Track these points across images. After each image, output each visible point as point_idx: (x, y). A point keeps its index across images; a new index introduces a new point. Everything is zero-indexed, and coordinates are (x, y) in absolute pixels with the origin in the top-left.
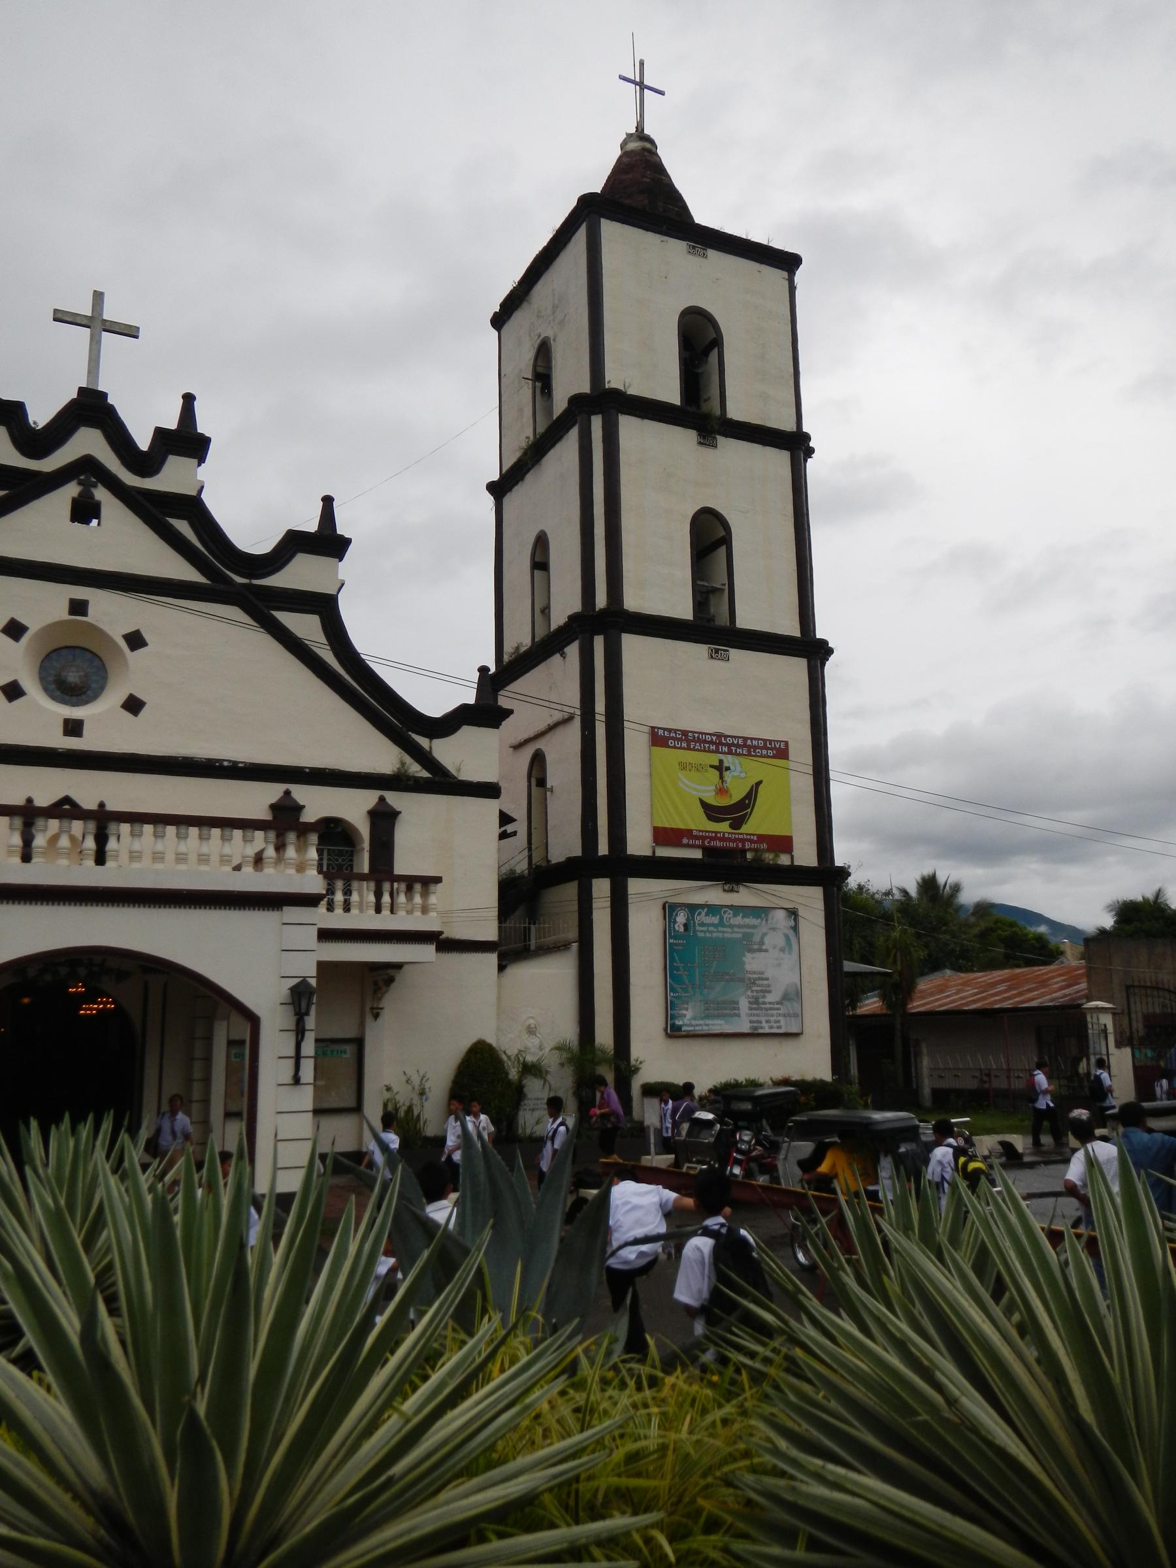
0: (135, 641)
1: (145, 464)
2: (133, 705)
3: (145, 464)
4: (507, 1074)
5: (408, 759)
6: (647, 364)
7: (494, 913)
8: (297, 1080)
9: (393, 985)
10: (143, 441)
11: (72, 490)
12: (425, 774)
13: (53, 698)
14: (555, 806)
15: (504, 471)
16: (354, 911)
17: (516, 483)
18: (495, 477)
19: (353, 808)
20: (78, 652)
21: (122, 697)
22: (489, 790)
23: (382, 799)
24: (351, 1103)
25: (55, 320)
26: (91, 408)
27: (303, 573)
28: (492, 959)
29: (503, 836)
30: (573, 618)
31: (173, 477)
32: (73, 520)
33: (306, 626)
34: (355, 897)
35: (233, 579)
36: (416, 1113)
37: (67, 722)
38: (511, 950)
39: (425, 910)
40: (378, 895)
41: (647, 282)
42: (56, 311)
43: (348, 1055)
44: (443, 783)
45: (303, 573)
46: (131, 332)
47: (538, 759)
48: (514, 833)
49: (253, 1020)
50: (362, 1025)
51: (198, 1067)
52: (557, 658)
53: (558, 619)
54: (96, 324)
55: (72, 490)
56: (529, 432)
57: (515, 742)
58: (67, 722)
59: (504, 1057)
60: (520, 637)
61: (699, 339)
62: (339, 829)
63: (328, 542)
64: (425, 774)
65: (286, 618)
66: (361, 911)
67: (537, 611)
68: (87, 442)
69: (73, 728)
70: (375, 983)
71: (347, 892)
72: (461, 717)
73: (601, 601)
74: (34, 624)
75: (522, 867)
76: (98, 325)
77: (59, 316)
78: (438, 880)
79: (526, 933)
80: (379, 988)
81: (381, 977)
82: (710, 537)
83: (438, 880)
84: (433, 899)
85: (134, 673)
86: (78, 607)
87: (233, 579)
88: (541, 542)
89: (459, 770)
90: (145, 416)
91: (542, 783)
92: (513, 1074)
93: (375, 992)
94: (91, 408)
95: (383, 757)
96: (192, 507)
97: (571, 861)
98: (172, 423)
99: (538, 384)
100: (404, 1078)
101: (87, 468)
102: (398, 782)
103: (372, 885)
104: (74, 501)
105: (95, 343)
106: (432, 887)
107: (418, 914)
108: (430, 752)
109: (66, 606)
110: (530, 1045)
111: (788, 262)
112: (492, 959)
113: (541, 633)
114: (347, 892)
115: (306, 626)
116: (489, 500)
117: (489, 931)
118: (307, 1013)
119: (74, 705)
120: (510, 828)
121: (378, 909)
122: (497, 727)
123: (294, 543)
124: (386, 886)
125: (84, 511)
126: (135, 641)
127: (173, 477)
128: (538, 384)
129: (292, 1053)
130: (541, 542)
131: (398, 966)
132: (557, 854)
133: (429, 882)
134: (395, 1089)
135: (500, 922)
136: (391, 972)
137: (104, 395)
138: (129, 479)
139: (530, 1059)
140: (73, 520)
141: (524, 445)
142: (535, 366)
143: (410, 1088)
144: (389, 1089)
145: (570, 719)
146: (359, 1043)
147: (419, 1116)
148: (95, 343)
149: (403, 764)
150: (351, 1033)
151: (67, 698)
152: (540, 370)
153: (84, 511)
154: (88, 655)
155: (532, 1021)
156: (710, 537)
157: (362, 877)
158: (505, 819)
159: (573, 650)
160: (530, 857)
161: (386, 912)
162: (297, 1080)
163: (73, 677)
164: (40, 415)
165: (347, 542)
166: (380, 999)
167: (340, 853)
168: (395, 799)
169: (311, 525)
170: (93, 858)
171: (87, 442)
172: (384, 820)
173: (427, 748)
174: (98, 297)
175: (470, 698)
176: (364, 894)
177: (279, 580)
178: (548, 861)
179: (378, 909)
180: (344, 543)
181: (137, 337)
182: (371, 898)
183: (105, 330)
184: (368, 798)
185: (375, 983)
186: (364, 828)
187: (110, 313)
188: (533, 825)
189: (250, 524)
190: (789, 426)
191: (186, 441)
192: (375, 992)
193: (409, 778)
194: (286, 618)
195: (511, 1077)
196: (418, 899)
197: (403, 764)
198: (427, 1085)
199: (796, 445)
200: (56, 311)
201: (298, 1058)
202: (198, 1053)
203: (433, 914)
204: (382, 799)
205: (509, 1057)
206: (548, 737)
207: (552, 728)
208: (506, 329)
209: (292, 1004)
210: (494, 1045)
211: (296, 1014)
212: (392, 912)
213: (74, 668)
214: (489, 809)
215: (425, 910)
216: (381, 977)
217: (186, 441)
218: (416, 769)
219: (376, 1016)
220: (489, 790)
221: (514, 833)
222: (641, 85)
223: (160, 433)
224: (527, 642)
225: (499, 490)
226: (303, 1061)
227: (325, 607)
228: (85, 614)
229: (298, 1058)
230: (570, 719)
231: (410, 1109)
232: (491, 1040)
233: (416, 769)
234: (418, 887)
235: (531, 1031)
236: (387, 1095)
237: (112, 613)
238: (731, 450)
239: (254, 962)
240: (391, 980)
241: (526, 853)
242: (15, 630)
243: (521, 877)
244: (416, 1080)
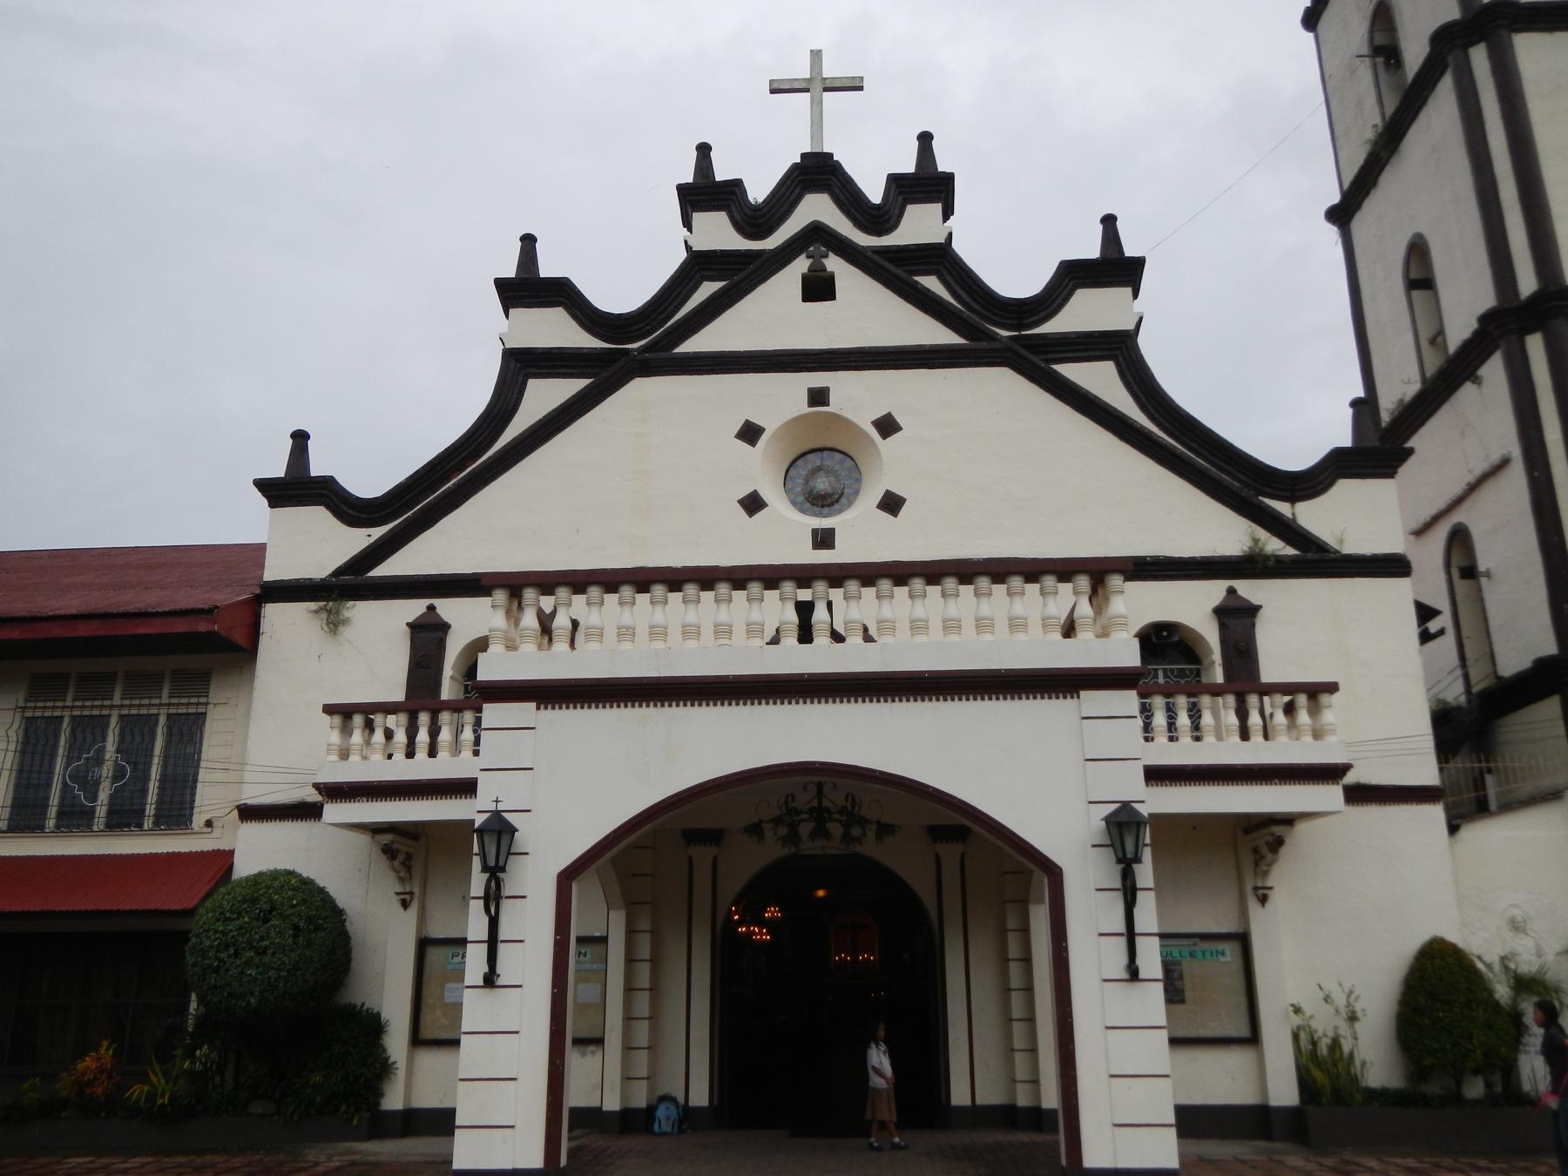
1: (878, 218)
2: (891, 504)
3: (878, 218)
4: (1491, 992)
5: (1262, 534)
7: (1428, 742)
8: (1133, 974)
9: (1284, 851)
10: (874, 192)
11: (801, 265)
12: (1290, 551)
13: (803, 511)
14: (1496, 597)
15: (1346, 185)
16: (1209, 739)
17: (1367, 194)
18: (1335, 198)
19: (1192, 606)
20: (826, 453)
21: (878, 496)
22: (1392, 566)
23: (1231, 591)
24: (1244, 1032)
25: (773, 91)
26: (817, 172)
27: (1089, 311)
28: (1435, 813)
29: (1426, 637)
30: (1486, 319)
31: (918, 225)
32: (805, 299)
33: (1101, 379)
34: (1207, 719)
35: (997, 332)
36: (1346, 1049)
37: (815, 532)
38: (1465, 801)
39: (1317, 734)
40: (1242, 714)
42: (771, 82)
43: (1228, 958)
44: (1317, 560)
45: (1089, 311)
46: (855, 86)
47: (1460, 539)
48: (1442, 632)
49: (1054, 873)
50: (1244, 914)
51: (1015, 969)
52: (1468, 389)
53: (1459, 329)
54: (819, 85)
56: (1378, 121)
57: (1415, 525)
58: (815, 532)
59: (1480, 966)
60: (1400, 383)
62: (1176, 639)
63: (1116, 268)
64: (1290, 551)
66: (1219, 738)
67: (1425, 344)
68: (817, 208)
69: (824, 539)
70: (1256, 851)
71: (1195, 713)
72: (1338, 466)
73: (1527, 283)
74: (770, 423)
75: (1455, 693)
76: (818, 86)
77: (775, 86)
78: (1332, 688)
79: (1479, 784)
80: (1262, 857)
81: (1260, 839)
83: (1332, 688)
84: (1328, 717)
85: (891, 465)
86: (818, 397)
87: (997, 332)
88: (1418, 250)
89: (1341, 541)
91: (1470, 572)
92: (1502, 992)
93: (1257, 863)
94: (817, 172)
95: (1222, 531)
96: (941, 257)
97: (1542, 665)
98: (907, 164)
99: (1380, 60)
100: (1321, 995)
101: (817, 235)
102: (1252, 566)
103: (1231, 699)
104: (805, 278)
105: (817, 106)
106: (1325, 699)
107: (1308, 739)
108: (1294, 520)
109: (804, 397)
110: (1520, 949)
112: (1435, 813)
113: (1433, 364)
114: (1195, 713)
115: (1101, 379)
116: (1332, 233)
117: (1426, 773)
118: (1137, 859)
119: (826, 516)
120: (1433, 626)
121: (1245, 735)
122: (1391, 475)
123: (1073, 276)
124: (1253, 700)
125: (818, 288)
126: (887, 426)
128: (1380, 60)
129: (1120, 927)
130: (1418, 250)
131: (1288, 820)
132: (1514, 658)
133: (1317, 692)
134: (1308, 1011)
135: (1440, 761)
136: (1278, 830)
137: (830, 155)
139: (1527, 964)
140: (805, 299)
141: (1370, 134)
142: (1371, 39)
143: (1330, 1009)
144: (1297, 1010)
145: (1504, 463)
146: (1243, 940)
147: (1351, 1055)
148: (817, 106)
149: (1256, 541)
150: (1226, 924)
151: (817, 509)
152: (1380, 39)
153: (818, 288)
154: (838, 456)
155: (1516, 912)
157: (1216, 691)
158: (1425, 613)
159: (1494, 370)
160: (1466, 677)
161: (1257, 738)
162: (1133, 974)
163: (822, 484)
164: (758, 191)
165: (1138, 264)
166: (1266, 874)
167: (1182, 673)
168: (1249, 589)
169: (1091, 250)
170: (795, 634)
171: (817, 208)
172: (1237, 619)
173: (1289, 515)
174: (816, 55)
175: (1345, 439)
176: (1220, 713)
177: (1058, 324)
178: (1499, 678)
179: (1245, 735)
180: (1138, 264)
181: (860, 88)
182: (1232, 719)
183: (826, 89)
184: (1213, 592)
185: (1256, 851)
186: (1210, 633)
187: (830, 70)
188: (1465, 633)
189: (1012, 266)
191: (928, 184)
192: (1257, 863)
193: (1267, 557)
195: (1497, 996)
196: (1303, 717)
197: (1256, 541)
198: (1358, 1007)
200: (771, 82)
201: (1131, 935)
202: (1014, 950)
203: (1331, 739)
204: (1231, 591)
205: (1489, 966)
206: (1468, 503)
207: (1473, 488)
208: (1325, 22)
209: (1112, 845)
210: (1461, 945)
211: (1119, 861)
212: (1266, 737)
213: (823, 470)
214: (1396, 595)
215: (1317, 734)
216: (1260, 839)
217: (928, 184)
218: (1275, 546)
219: (1263, 900)
220: (1392, 566)
221: (1442, 632)
223: (895, 181)
224: (1413, 389)
225: (1341, 216)
226: (1139, 941)
227: (1119, 347)
228: (827, 404)
229: (1131, 935)
230: (1504, 463)
231: (1335, 1044)
232: (1453, 937)
233: (1275, 546)
234: (1302, 699)
235: (1517, 926)
236: (1297, 1020)
239: (1044, 778)
240: (1279, 843)
241: (1459, 672)
243: (1458, 709)
244: (1340, 1000)
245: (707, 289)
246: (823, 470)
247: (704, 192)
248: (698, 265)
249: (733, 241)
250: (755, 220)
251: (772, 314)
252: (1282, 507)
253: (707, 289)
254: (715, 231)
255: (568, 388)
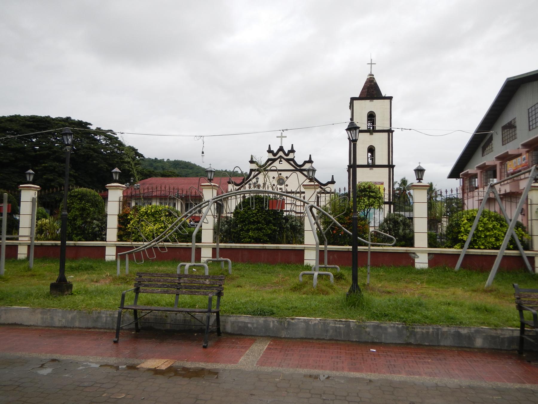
0: (287, 178)
6: (362, 123)
11: (279, 160)
26: (281, 149)
27: (307, 166)
31: (291, 156)
35: (298, 168)
41: (364, 107)
44: (326, 192)
45: (307, 166)
55: (279, 160)
61: (371, 117)
63: (310, 161)
65: (304, 172)
68: (281, 153)
82: (371, 150)
87: (298, 168)
90: (287, 149)
94: (281, 149)
96: (293, 160)
98: (290, 149)
101: (281, 157)
105: (282, 139)
111: (390, 98)
123: (305, 162)
127: (291, 156)
138: (285, 157)
148: (282, 139)
153: (281, 161)
156: (371, 150)
163: (281, 182)
164: (275, 151)
169: (308, 159)
190: (387, 127)
191: (292, 151)
194: (304, 172)
199: (390, 132)
217: (292, 151)
222: (371, 64)
237: (284, 174)
238: (375, 134)
242: (274, 178)
245: (270, 162)
246: (281, 181)
247: (270, 151)
248: (269, 160)
249: (272, 157)
250: (275, 155)
251: (276, 164)
252: (323, 187)
253: (270, 162)
254: (271, 156)
255: (257, 172)
